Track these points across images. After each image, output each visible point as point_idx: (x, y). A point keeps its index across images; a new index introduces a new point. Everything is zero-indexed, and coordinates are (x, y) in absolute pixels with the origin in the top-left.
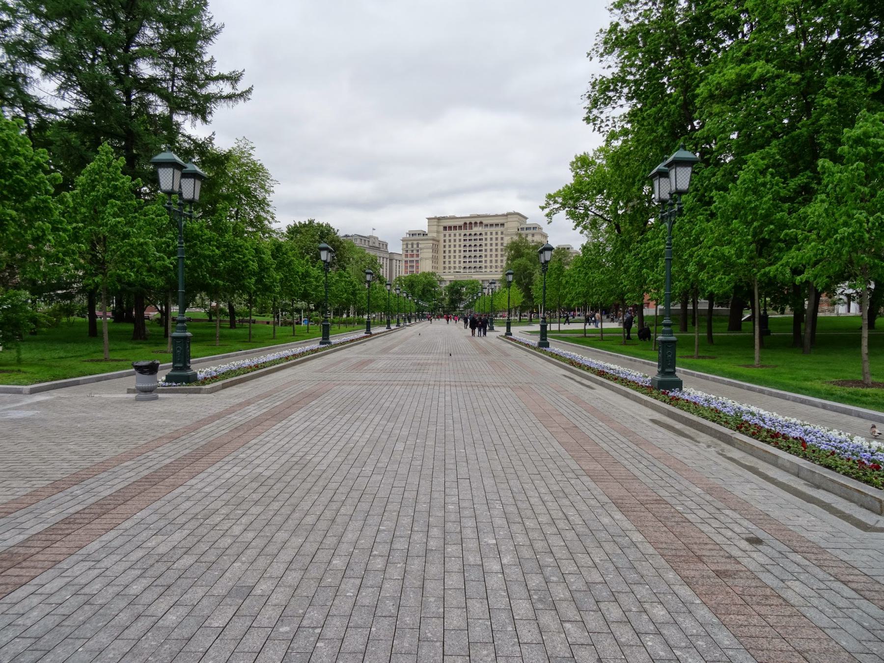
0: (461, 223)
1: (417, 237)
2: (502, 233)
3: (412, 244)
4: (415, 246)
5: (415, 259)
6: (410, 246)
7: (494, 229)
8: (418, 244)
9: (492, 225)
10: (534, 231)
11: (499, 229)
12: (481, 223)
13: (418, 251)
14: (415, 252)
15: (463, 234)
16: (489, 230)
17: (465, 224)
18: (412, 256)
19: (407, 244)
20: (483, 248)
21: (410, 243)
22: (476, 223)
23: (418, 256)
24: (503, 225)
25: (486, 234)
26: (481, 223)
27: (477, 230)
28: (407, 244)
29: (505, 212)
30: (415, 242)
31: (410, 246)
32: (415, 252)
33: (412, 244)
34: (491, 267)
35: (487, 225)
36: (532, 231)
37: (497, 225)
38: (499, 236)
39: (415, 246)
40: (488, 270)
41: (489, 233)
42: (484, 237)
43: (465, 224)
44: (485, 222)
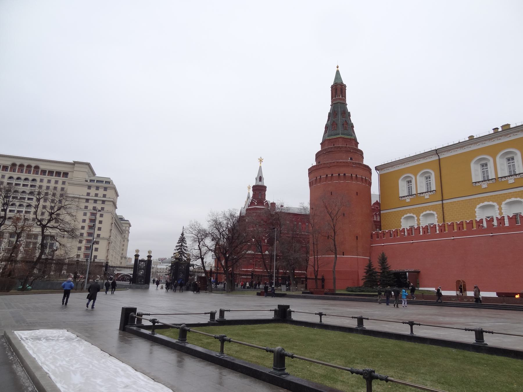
0: (8, 163)
2: (64, 183)
12: (37, 167)
15: (7, 176)
16: (46, 178)
25: (42, 180)
26: (37, 167)
29: (71, 161)
35: (44, 172)
43: (14, 165)
44: (42, 167)
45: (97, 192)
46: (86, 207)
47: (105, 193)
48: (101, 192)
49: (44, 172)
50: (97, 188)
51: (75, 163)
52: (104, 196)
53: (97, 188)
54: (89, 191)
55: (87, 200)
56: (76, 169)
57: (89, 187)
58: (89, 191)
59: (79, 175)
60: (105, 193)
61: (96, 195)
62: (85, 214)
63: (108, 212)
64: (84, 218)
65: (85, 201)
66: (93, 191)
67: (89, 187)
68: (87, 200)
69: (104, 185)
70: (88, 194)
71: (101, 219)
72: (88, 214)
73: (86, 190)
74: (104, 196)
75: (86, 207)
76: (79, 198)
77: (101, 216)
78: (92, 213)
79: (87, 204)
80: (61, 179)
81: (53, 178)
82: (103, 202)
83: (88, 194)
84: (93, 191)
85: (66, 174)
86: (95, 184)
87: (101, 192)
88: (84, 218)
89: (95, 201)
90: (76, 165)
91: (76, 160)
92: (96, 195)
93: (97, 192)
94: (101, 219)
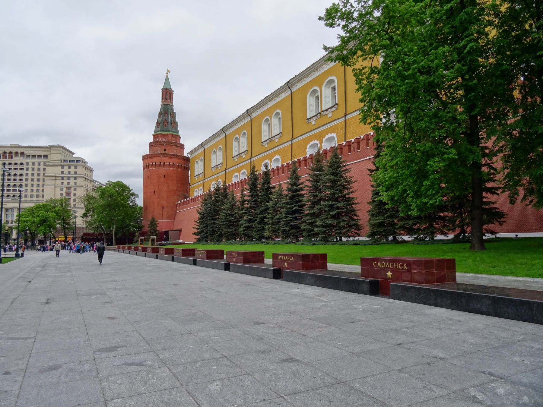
7: (36, 160)
9: (34, 156)
10: (78, 164)
11: (42, 160)
12: (22, 153)
16: (30, 160)
17: (5, 153)
20: (24, 178)
22: (17, 153)
24: (46, 156)
25: (28, 164)
26: (22, 153)
27: (18, 159)
34: (32, 196)
35: (28, 156)
36: (75, 164)
37: (40, 156)
38: (42, 167)
40: (29, 199)
41: (30, 163)
42: (25, 167)
43: (5, 153)
44: (27, 152)
45: (69, 170)
46: (62, 183)
47: (76, 170)
48: (72, 170)
49: (28, 156)
50: (69, 167)
51: (50, 147)
52: (76, 173)
53: (69, 167)
54: (63, 170)
55: (62, 178)
56: (52, 152)
57: (63, 167)
58: (63, 170)
59: (55, 157)
60: (76, 170)
61: (69, 173)
62: (62, 189)
63: (80, 186)
64: (62, 192)
65: (60, 178)
66: (66, 170)
67: (63, 167)
68: (62, 178)
69: (75, 164)
70: (63, 173)
71: (75, 192)
72: (65, 189)
73: (59, 170)
74: (76, 173)
75: (62, 183)
76: (56, 177)
77: (75, 189)
78: (67, 188)
79: (62, 181)
82: (75, 178)
83: (63, 173)
84: (66, 170)
86: (68, 163)
87: (72, 170)
88: (62, 192)
89: (69, 178)
90: (52, 148)
91: (51, 145)
92: (69, 173)
93: (69, 170)
94: (75, 192)
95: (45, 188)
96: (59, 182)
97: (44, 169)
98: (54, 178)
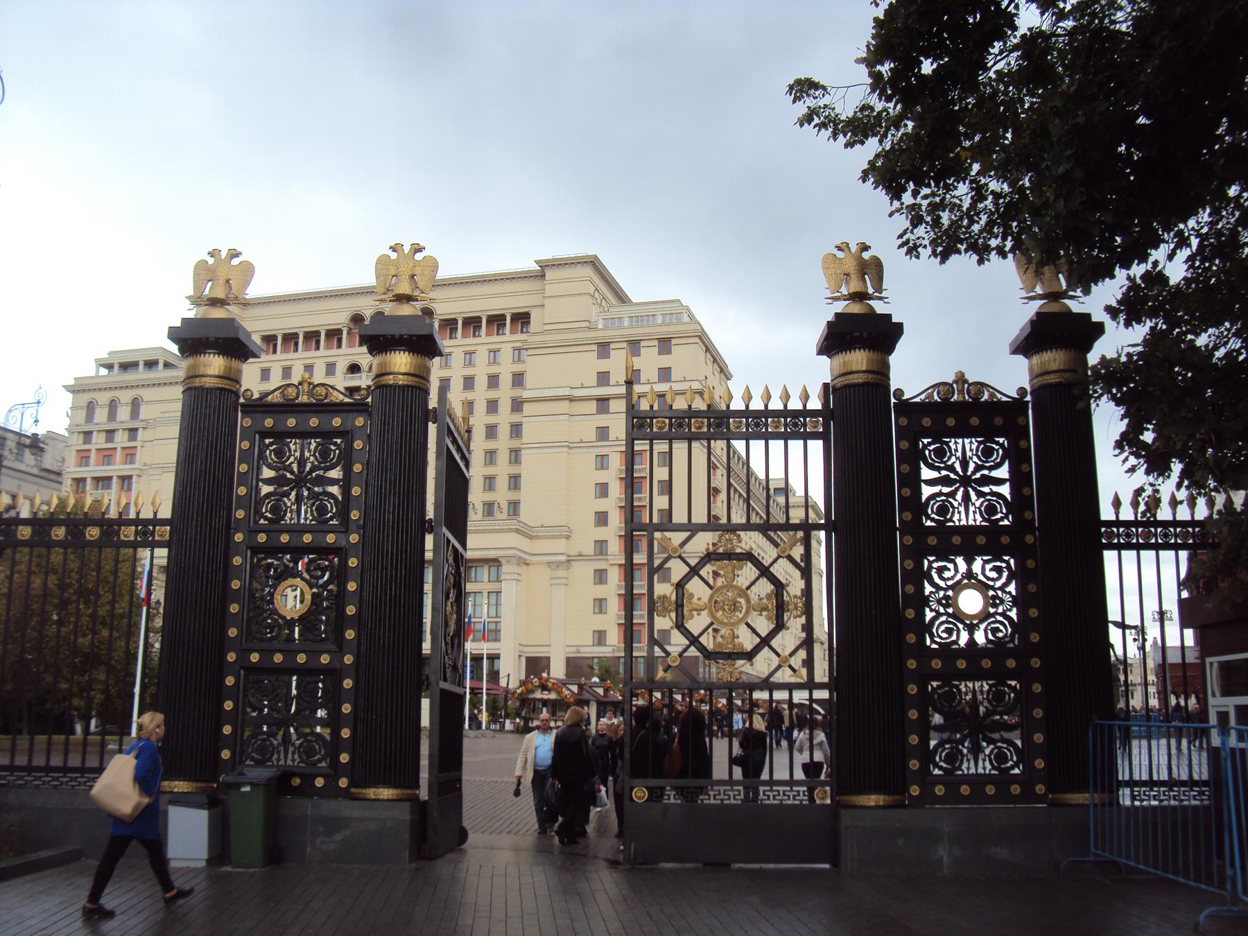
0: (338, 317)
1: (141, 374)
3: (113, 406)
4: (124, 413)
5: (117, 468)
6: (101, 415)
8: (135, 404)
13: (133, 432)
14: (121, 439)
18: (107, 456)
19: (91, 408)
21: (103, 398)
23: (130, 454)
28: (91, 408)
29: (528, 264)
30: (126, 397)
31: (101, 415)
32: (121, 439)
33: (113, 406)
39: (124, 413)
46: (603, 433)
47: (665, 361)
51: (545, 266)
54: (603, 365)
56: (550, 289)
57: (604, 349)
58: (603, 365)
60: (665, 361)
67: (604, 349)
73: (590, 364)
79: (603, 420)
80: (508, 339)
81: (484, 341)
83: (603, 378)
85: (522, 319)
90: (550, 274)
91: (547, 255)
95: (530, 465)
96: (587, 429)
97: (518, 379)
98: (564, 406)
